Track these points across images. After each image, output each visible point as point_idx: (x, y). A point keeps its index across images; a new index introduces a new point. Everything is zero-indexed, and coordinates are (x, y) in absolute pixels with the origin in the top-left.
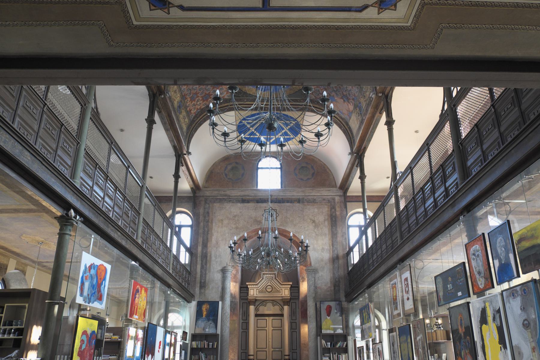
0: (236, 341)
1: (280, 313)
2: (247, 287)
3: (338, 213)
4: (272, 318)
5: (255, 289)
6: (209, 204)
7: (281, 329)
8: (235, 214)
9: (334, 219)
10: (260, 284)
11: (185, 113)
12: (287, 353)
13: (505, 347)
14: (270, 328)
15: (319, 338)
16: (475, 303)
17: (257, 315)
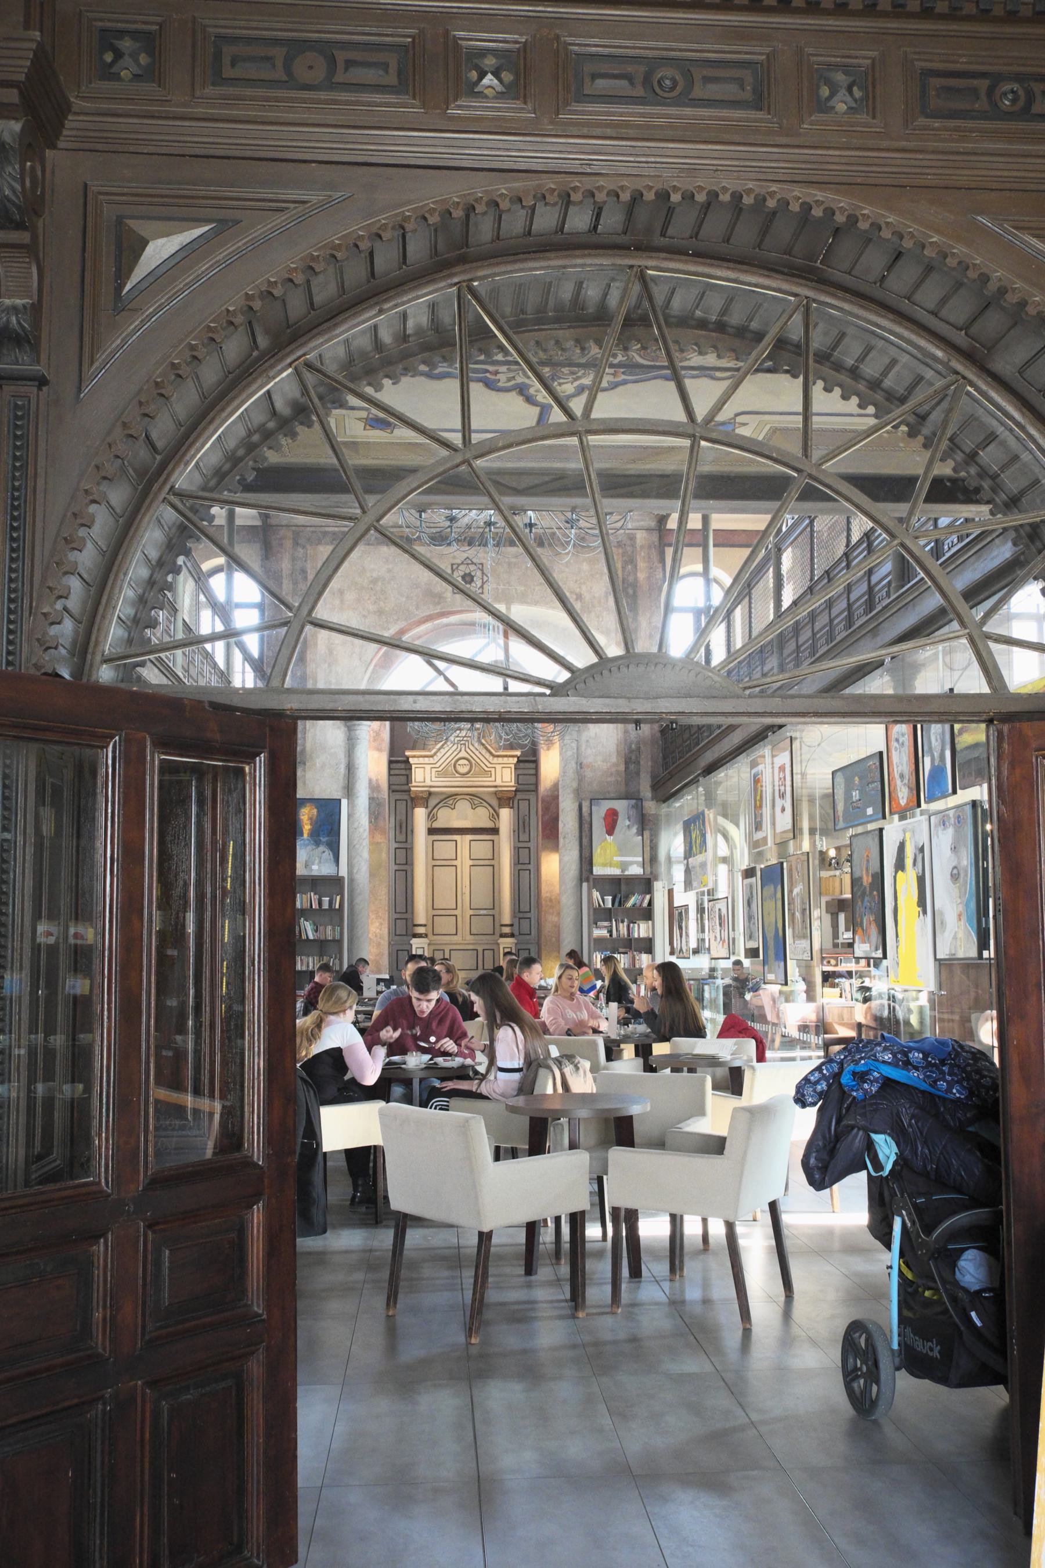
0: (383, 895)
1: (489, 825)
2: (407, 761)
3: (641, 576)
4: (469, 837)
5: (428, 767)
6: (304, 547)
7: (492, 863)
8: (375, 575)
9: (631, 591)
10: (439, 755)
12: (507, 919)
13: (925, 912)
14: (464, 863)
15: (585, 885)
16: (893, 830)
17: (431, 831)
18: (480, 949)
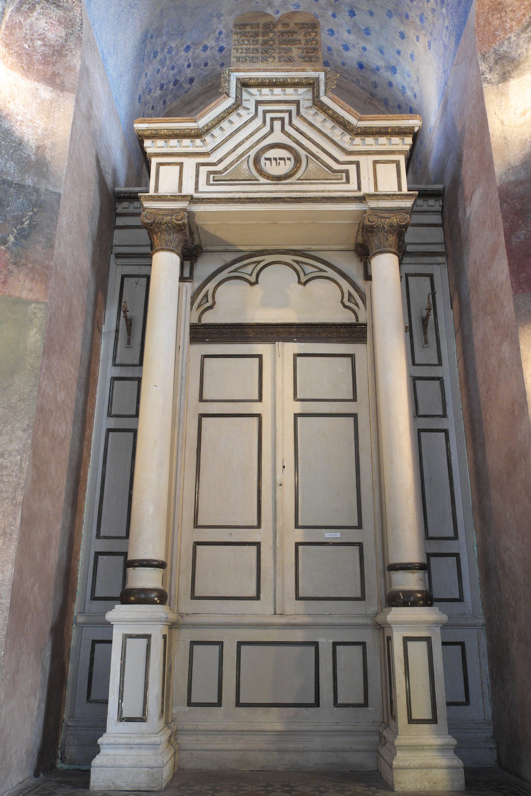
1: (344, 317)
4: (292, 348)
5: (190, 164)
10: (218, 134)
12: (408, 546)
14: (280, 406)
17: (200, 333)
18: (325, 642)
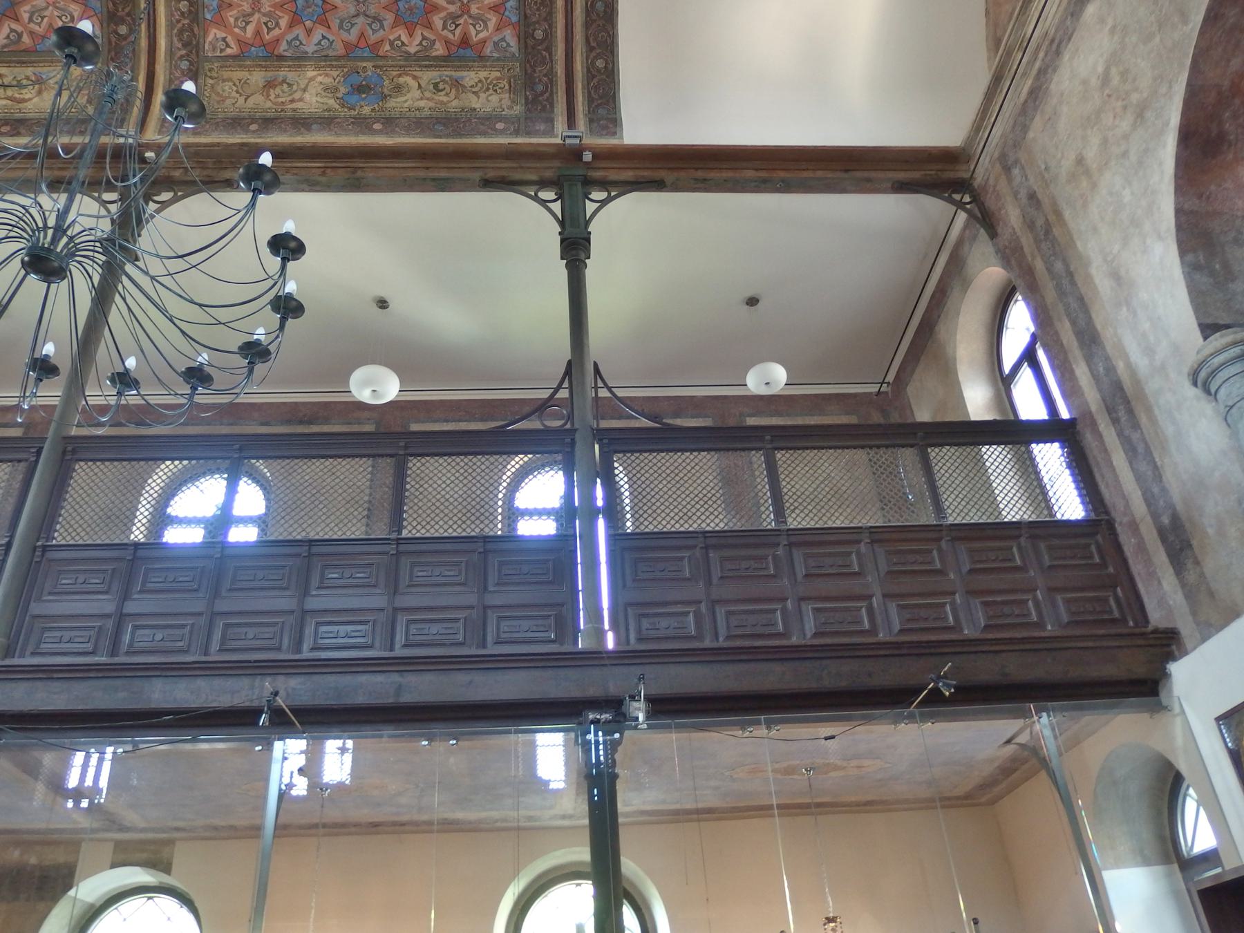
11: (428, 76)
